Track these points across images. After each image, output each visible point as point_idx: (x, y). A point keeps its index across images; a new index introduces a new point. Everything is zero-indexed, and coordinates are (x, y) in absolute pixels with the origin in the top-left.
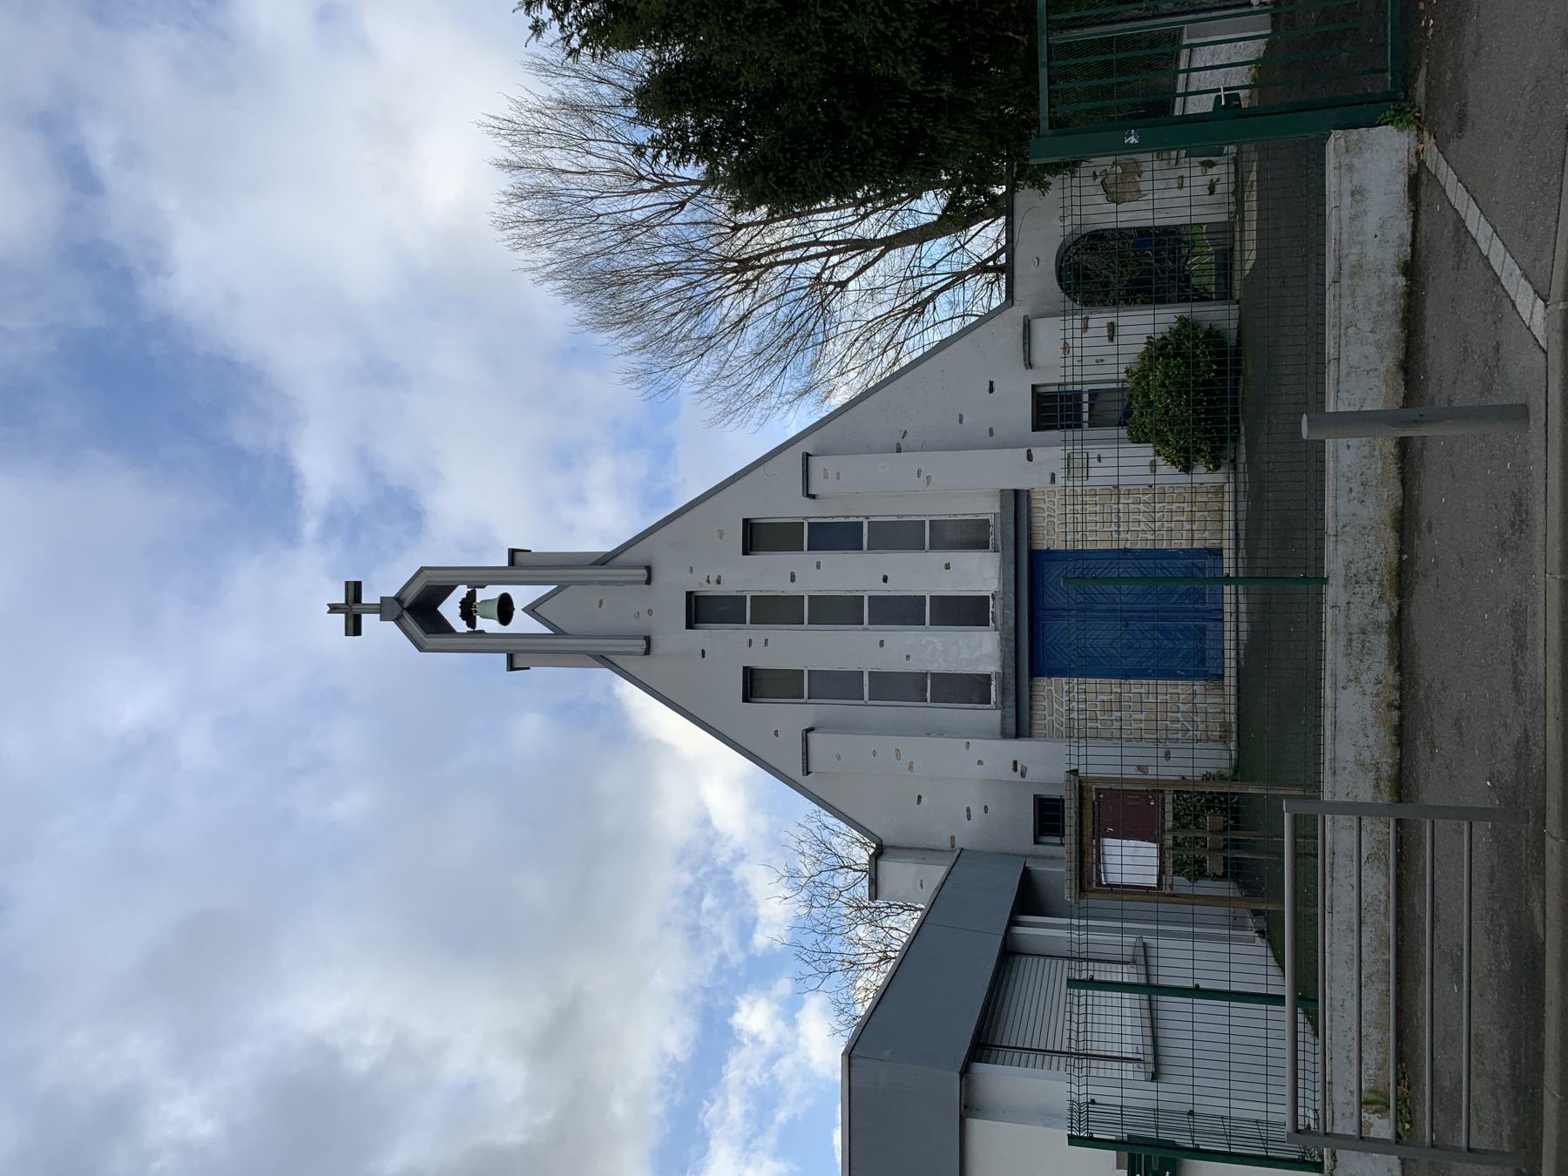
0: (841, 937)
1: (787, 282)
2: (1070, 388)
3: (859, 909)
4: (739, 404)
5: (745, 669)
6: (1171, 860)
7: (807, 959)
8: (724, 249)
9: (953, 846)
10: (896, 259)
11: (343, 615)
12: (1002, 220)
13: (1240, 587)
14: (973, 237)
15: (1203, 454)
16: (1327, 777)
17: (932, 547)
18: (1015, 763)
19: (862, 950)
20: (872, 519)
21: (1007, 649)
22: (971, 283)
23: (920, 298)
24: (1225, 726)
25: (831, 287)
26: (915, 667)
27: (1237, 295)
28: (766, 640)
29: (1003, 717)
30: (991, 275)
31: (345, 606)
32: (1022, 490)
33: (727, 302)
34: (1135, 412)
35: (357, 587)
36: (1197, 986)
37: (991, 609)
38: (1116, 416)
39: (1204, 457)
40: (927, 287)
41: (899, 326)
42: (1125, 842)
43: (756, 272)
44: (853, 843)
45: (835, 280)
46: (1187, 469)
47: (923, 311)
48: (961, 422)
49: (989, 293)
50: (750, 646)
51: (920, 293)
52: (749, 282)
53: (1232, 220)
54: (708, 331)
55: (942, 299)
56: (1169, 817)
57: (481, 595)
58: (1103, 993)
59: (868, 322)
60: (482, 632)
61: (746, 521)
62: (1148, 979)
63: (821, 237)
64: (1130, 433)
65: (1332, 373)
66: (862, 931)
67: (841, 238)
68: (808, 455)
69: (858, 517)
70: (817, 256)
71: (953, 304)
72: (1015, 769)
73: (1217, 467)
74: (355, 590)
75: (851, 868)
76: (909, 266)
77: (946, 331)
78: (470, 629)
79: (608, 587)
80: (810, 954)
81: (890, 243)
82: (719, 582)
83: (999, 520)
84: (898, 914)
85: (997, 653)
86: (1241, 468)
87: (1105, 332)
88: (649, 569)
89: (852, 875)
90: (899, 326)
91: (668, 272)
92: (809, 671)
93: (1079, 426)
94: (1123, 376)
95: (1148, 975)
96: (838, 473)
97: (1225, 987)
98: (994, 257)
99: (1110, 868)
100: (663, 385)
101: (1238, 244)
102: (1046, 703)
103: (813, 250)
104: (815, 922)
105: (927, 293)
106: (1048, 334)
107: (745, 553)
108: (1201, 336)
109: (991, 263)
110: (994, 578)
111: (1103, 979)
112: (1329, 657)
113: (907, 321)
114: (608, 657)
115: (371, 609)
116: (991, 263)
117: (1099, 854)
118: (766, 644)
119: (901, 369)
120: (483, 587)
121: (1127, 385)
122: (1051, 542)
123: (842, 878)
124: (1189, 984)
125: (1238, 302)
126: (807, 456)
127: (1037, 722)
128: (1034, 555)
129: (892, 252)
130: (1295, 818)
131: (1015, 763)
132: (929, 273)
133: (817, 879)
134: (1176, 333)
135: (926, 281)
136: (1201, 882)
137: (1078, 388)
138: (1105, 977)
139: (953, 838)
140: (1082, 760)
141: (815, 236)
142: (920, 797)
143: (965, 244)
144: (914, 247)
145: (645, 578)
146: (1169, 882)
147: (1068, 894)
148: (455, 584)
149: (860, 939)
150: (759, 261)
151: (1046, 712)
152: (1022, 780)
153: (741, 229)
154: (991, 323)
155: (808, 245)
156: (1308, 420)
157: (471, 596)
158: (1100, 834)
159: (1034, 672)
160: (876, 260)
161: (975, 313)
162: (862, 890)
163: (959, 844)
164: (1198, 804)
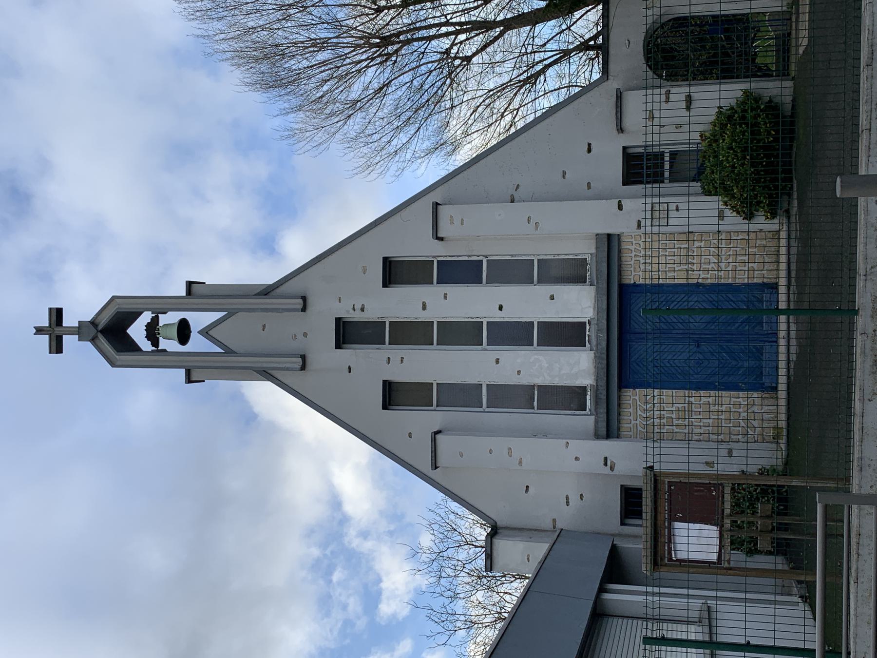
1: (421, 56)
3: (479, 578)
4: (378, 158)
5: (385, 382)
6: (729, 540)
7: (437, 620)
8: (370, 28)
9: (554, 527)
11: (48, 336)
12: (600, 7)
13: (791, 317)
14: (578, 20)
15: (762, 205)
17: (539, 282)
18: (606, 459)
19: (482, 611)
20: (490, 258)
21: (600, 366)
22: (575, 58)
23: (532, 71)
27: (793, 74)
28: (402, 358)
29: (596, 422)
30: (592, 53)
31: (49, 329)
32: (615, 234)
33: (371, 72)
34: (708, 170)
35: (59, 312)
36: (749, 642)
37: (587, 333)
38: (693, 173)
40: (540, 62)
41: (515, 94)
43: (396, 47)
44: (474, 524)
45: (461, 55)
46: (749, 216)
48: (564, 177)
49: (590, 67)
50: (389, 363)
51: (533, 67)
52: (389, 55)
54: (354, 96)
55: (550, 72)
57: (163, 319)
58: (674, 649)
59: (490, 91)
60: (164, 351)
61: (385, 259)
62: (711, 637)
63: (451, 18)
65: (864, 141)
66: (480, 595)
67: (467, 20)
68: (437, 204)
70: (447, 34)
72: (606, 464)
73: (774, 215)
74: (57, 315)
75: (473, 545)
76: (524, 45)
77: (552, 100)
78: (154, 348)
80: (439, 615)
81: (508, 25)
82: (362, 310)
84: (512, 582)
85: (592, 370)
86: (793, 219)
88: (304, 299)
89: (473, 550)
90: (515, 94)
91: (320, 45)
92: (437, 384)
93: (662, 182)
95: (711, 633)
96: (462, 219)
98: (595, 38)
99: (679, 547)
100: (316, 142)
102: (631, 410)
103: (444, 29)
105: (539, 67)
106: (635, 102)
107: (385, 285)
108: (762, 107)
109: (592, 43)
110: (590, 307)
112: (858, 374)
113: (522, 91)
114: (269, 372)
115: (71, 331)
116: (592, 43)
117: (671, 535)
118: (402, 361)
120: (165, 313)
124: (742, 641)
125: (793, 79)
126: (436, 205)
127: (625, 426)
128: (622, 287)
129: (510, 32)
130: (826, 508)
131: (606, 459)
132: (541, 50)
133: (445, 554)
134: (742, 103)
135: (538, 57)
136: (757, 558)
138: (677, 635)
139: (554, 520)
141: (446, 17)
142: (527, 487)
143: (571, 26)
145: (301, 307)
146: (727, 558)
147: (645, 567)
149: (480, 603)
150: (399, 38)
151: (631, 418)
153: (383, 11)
155: (441, 25)
157: (155, 321)
158: (673, 519)
159: (621, 386)
160: (496, 38)
161: (579, 84)
162: (481, 563)
163: (559, 525)
164: (755, 493)
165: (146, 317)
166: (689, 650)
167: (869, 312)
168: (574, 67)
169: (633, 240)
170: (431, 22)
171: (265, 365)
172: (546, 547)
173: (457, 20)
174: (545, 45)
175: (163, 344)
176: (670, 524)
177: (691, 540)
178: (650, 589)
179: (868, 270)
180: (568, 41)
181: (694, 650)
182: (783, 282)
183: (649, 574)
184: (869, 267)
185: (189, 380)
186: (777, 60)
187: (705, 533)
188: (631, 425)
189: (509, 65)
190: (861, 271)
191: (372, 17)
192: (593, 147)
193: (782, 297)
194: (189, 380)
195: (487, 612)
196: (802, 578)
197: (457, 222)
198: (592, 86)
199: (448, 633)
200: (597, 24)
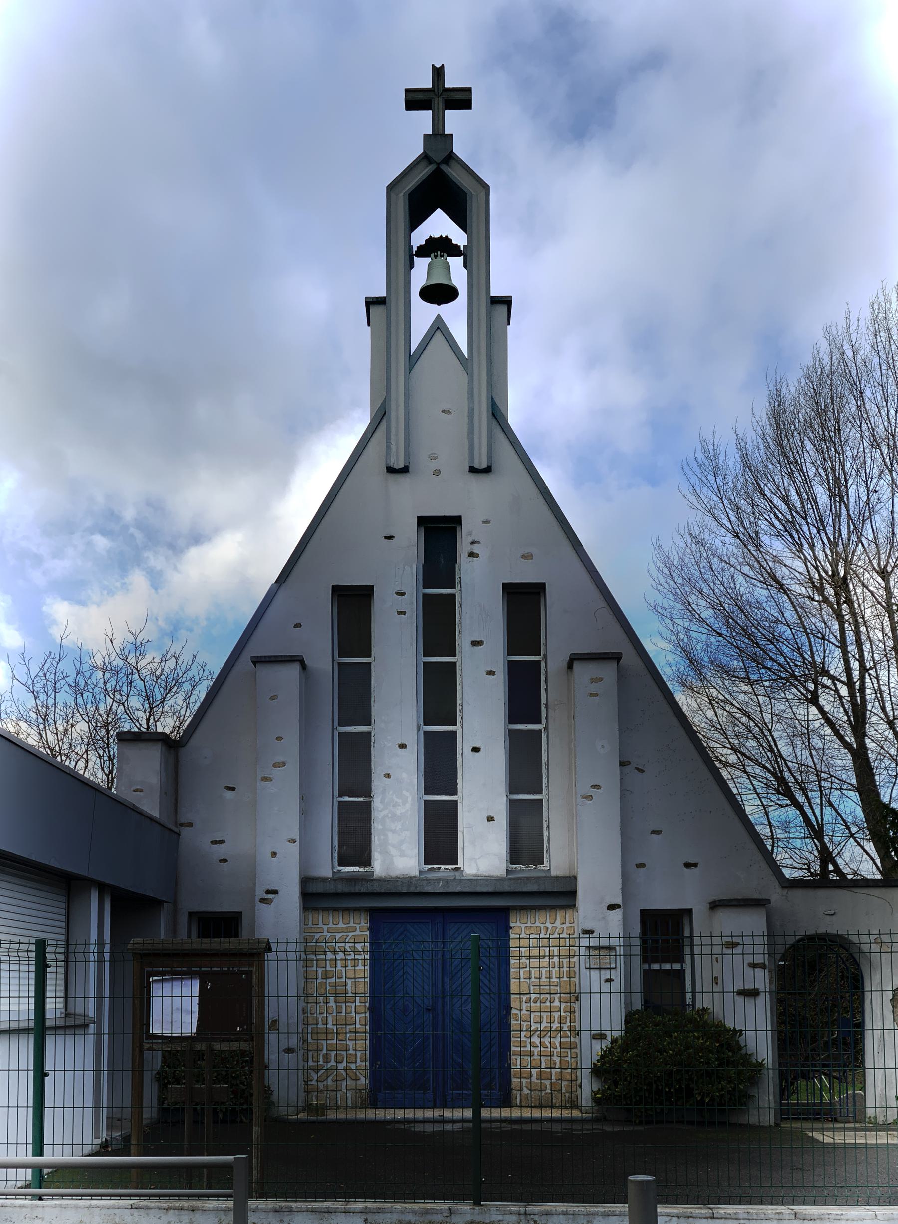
0: (73, 704)
1: (819, 635)
2: (687, 950)
3: (106, 725)
6: (179, 1049)
7: (46, 667)
8: (860, 560)
9: (182, 825)
10: (843, 760)
11: (430, 86)
13: (472, 1124)
14: (862, 847)
16: (271, 1204)
18: (275, 892)
19: (61, 728)
21: (399, 883)
23: (795, 789)
24: (321, 1109)
25: (811, 686)
26: (378, 783)
28: (404, 613)
29: (324, 880)
30: (817, 868)
31: (440, 87)
32: (575, 900)
33: (799, 565)
34: (659, 1018)
36: (47, 1075)
37: (443, 867)
39: (609, 1088)
40: (807, 797)
41: (764, 767)
42: (196, 1000)
43: (832, 599)
44: (178, 717)
46: (596, 1071)
47: (779, 793)
49: (797, 866)
50: (398, 594)
51: (801, 789)
52: (821, 590)
53: (867, 1120)
54: (765, 539)
55: (793, 812)
56: (225, 1046)
57: (457, 263)
58: (33, 982)
59: (770, 731)
60: (412, 266)
62: (51, 1028)
63: (869, 675)
64: (637, 1012)
67: (868, 697)
69: (547, 718)
70: (848, 670)
71: (786, 826)
75: (150, 715)
76: (831, 776)
78: (415, 249)
79: (467, 420)
81: (860, 756)
82: (472, 555)
83: (543, 875)
84: (103, 769)
85: (394, 873)
87: (749, 986)
88: (488, 470)
89: (142, 716)
90: (764, 767)
94: (699, 1006)
95: (55, 1028)
96: (597, 695)
97: (48, 1102)
98: (837, 870)
99: (167, 986)
101: (841, 1125)
102: (341, 925)
103: (855, 665)
104: (87, 675)
105: (800, 798)
107: (507, 587)
109: (831, 868)
110: (478, 870)
111: (48, 982)
113: (769, 775)
114: (384, 421)
115: (439, 122)
116: (831, 868)
118: (400, 613)
119: (717, 769)
120: (465, 266)
121: (689, 1010)
122: (518, 931)
123: (139, 705)
124: (49, 1066)
125: (777, 1125)
126: (616, 657)
129: (850, 757)
132: (824, 799)
133: (136, 676)
135: (815, 795)
136: (156, 1086)
137: (688, 959)
138: (50, 979)
139: (190, 825)
140: (282, 956)
141: (871, 668)
143: (855, 839)
144: (854, 781)
145: (477, 466)
147: (136, 942)
148: (468, 268)
149: (73, 725)
150: (844, 602)
151: (331, 925)
152: (257, 899)
153: (883, 580)
154: (764, 865)
156: (649, 1181)
157: (451, 249)
160: (841, 738)
161: (775, 851)
162: (126, 726)
163: (185, 832)
164: (239, 1082)
165: (459, 237)
166: (32, 1000)
167: (478, 1218)
168: (798, 844)
169: (568, 925)
170: (866, 647)
171: (393, 414)
172: (156, 814)
173: (868, 684)
174: (831, 805)
175: (422, 264)
176: (195, 973)
177: (177, 1001)
178: (107, 948)
179: (532, 1216)
180: (834, 834)
181: (32, 1007)
182: (516, 1113)
183: (129, 946)
184: (536, 1218)
185: (370, 303)
186: (803, 1105)
187: (187, 1019)
188: (321, 925)
189: (804, 756)
190: (529, 1209)
191: (875, 562)
192: (692, 870)
193: (496, 1113)
194: (370, 303)
195: (61, 736)
196: (133, 1142)
197: (593, 688)
198: (775, 868)
199: (30, 682)
200: (855, 874)
